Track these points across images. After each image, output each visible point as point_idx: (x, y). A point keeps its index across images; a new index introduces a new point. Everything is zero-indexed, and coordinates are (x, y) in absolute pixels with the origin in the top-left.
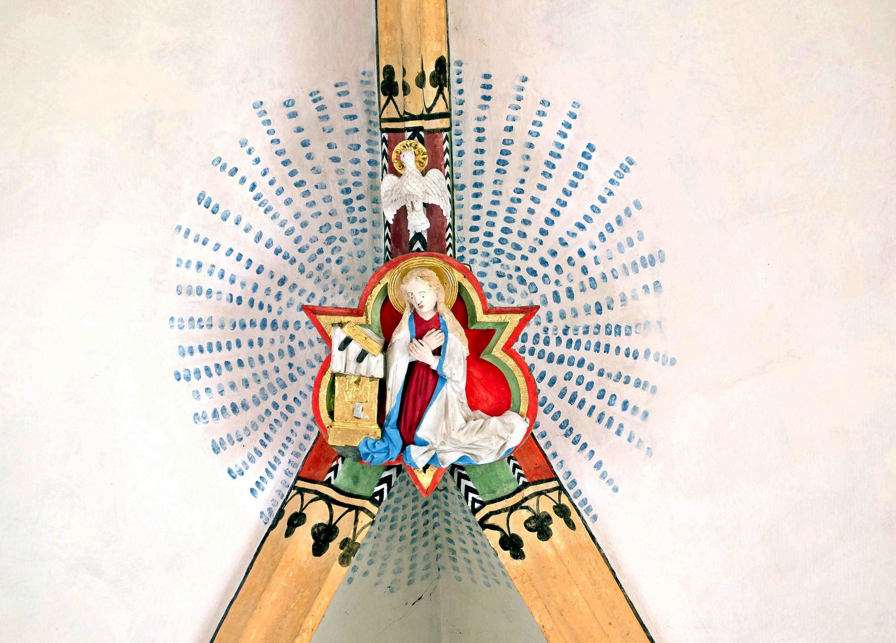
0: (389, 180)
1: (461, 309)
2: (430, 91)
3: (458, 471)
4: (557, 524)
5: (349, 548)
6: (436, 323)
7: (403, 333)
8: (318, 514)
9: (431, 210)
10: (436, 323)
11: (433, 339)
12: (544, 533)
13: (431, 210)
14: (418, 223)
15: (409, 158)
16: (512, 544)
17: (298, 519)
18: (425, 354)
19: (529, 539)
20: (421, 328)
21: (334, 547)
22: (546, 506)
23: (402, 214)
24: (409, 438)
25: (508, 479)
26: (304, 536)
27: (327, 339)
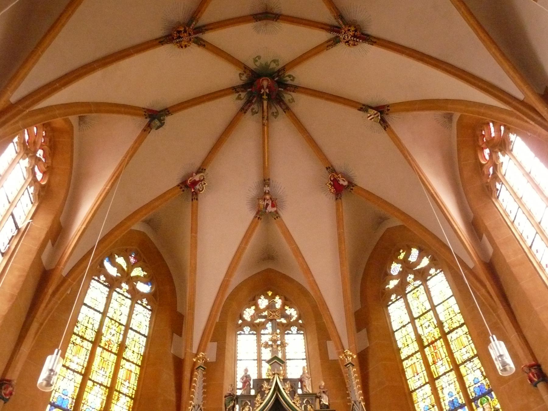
0: (265, 188)
1: (271, 199)
2: (268, 181)
3: (270, 212)
4: (278, 217)
5: (261, 219)
6: (269, 200)
7: (266, 201)
8: (258, 216)
9: (268, 191)
10: (269, 200)
11: (268, 201)
12: (278, 218)
13: (268, 191)
14: (267, 192)
15: (266, 186)
16: (275, 219)
17: (257, 217)
18: (268, 202)
19: (276, 219)
20: (267, 200)
21: (260, 219)
22: (278, 216)
23: (266, 191)
24: (266, 209)
25: (275, 213)
26: (257, 218)
27: (259, 201)
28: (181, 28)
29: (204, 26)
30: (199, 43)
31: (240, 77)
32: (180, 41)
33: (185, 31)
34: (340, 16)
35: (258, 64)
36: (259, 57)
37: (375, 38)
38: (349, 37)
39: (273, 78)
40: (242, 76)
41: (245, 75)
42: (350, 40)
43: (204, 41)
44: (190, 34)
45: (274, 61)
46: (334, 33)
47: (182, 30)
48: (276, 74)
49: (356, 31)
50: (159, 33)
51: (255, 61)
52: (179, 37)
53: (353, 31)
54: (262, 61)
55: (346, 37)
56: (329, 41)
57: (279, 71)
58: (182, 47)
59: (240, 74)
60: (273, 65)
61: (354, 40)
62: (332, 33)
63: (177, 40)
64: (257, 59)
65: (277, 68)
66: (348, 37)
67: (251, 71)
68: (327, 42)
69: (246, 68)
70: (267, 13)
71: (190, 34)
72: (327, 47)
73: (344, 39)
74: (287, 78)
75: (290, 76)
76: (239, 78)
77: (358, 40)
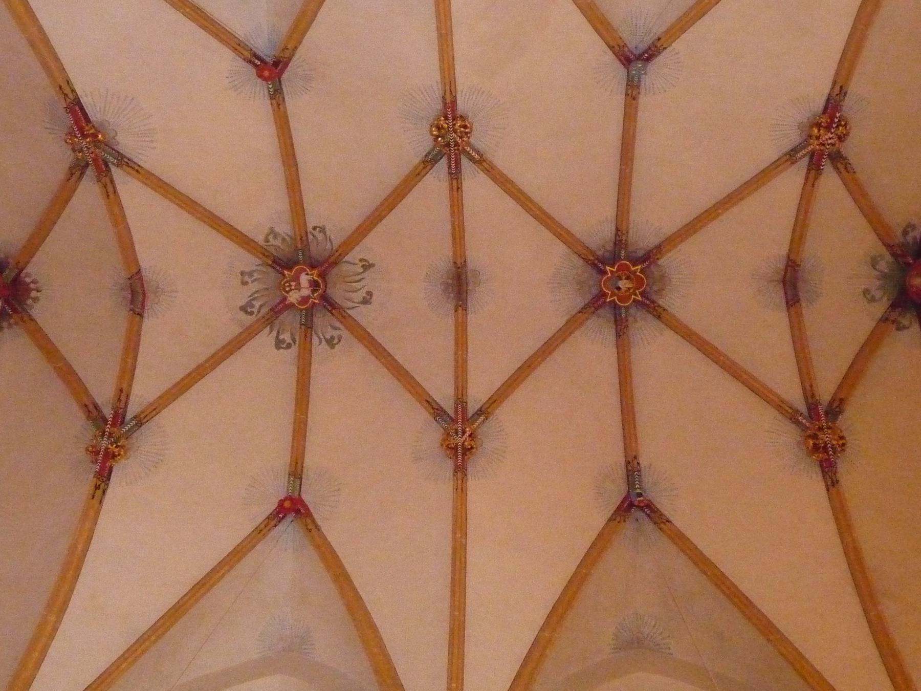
28: (809, 444)
29: (806, 398)
30: (837, 409)
31: (904, 328)
32: (832, 448)
33: (815, 437)
34: (791, 156)
35: (878, 294)
36: (866, 292)
37: (832, 88)
38: (831, 136)
39: (908, 264)
40: (901, 325)
41: (900, 319)
42: (837, 135)
43: (833, 400)
44: (821, 429)
45: (874, 263)
46: (823, 164)
47: (811, 443)
48: (900, 259)
49: (819, 126)
50: (814, 484)
51: (873, 300)
52: (825, 448)
53: (819, 130)
54: (874, 284)
55: (829, 142)
56: (836, 168)
57: (893, 255)
58: (844, 445)
59: (898, 329)
60: (883, 266)
61: (837, 127)
62: (822, 168)
63: (830, 452)
64: (868, 296)
65: (888, 257)
66: (830, 138)
67: (893, 306)
68: (839, 173)
69: (884, 320)
70: (784, 281)
71: (821, 429)
72: (848, 172)
73: (833, 145)
74: (910, 238)
75: (905, 233)
76: (905, 332)
77: (836, 120)
